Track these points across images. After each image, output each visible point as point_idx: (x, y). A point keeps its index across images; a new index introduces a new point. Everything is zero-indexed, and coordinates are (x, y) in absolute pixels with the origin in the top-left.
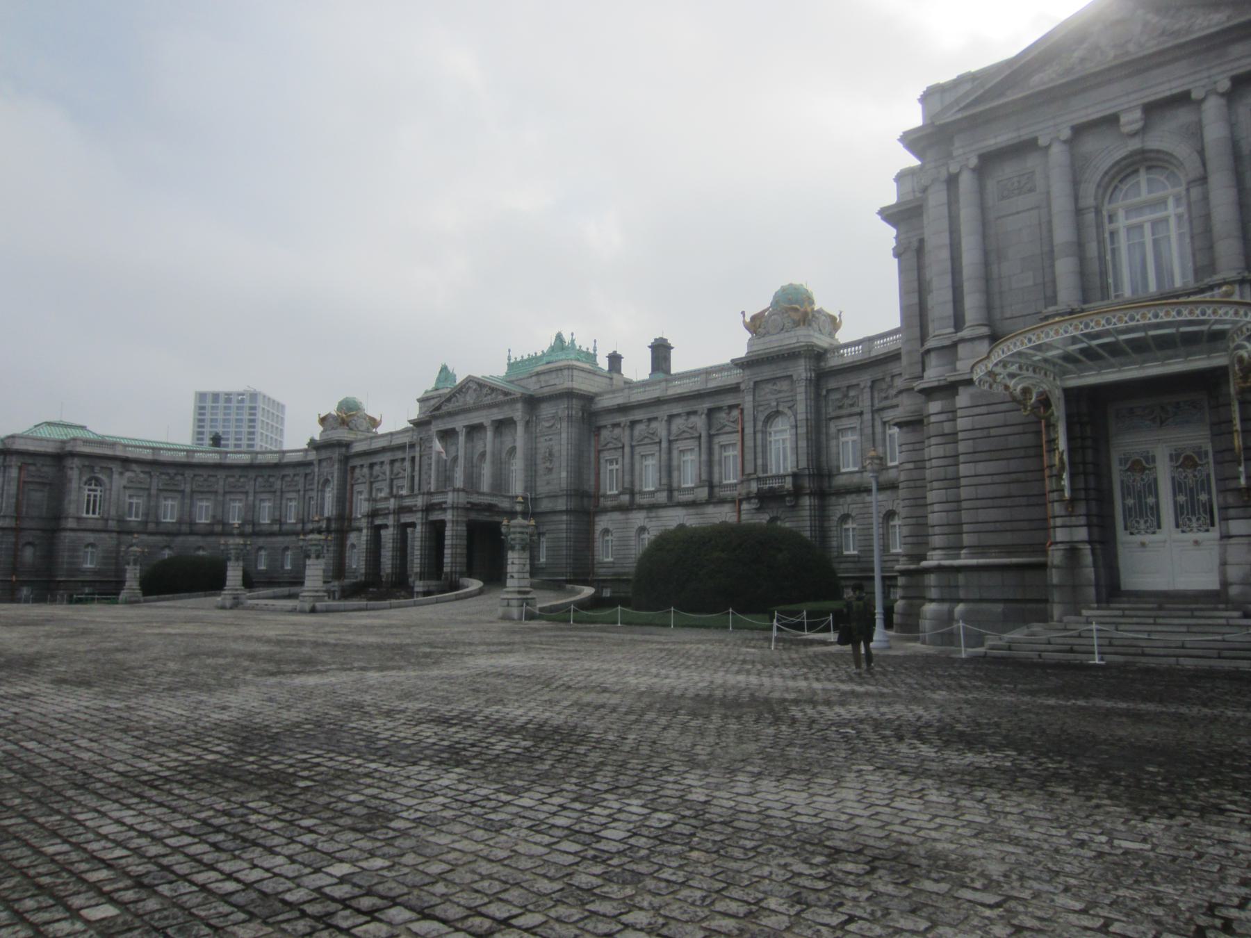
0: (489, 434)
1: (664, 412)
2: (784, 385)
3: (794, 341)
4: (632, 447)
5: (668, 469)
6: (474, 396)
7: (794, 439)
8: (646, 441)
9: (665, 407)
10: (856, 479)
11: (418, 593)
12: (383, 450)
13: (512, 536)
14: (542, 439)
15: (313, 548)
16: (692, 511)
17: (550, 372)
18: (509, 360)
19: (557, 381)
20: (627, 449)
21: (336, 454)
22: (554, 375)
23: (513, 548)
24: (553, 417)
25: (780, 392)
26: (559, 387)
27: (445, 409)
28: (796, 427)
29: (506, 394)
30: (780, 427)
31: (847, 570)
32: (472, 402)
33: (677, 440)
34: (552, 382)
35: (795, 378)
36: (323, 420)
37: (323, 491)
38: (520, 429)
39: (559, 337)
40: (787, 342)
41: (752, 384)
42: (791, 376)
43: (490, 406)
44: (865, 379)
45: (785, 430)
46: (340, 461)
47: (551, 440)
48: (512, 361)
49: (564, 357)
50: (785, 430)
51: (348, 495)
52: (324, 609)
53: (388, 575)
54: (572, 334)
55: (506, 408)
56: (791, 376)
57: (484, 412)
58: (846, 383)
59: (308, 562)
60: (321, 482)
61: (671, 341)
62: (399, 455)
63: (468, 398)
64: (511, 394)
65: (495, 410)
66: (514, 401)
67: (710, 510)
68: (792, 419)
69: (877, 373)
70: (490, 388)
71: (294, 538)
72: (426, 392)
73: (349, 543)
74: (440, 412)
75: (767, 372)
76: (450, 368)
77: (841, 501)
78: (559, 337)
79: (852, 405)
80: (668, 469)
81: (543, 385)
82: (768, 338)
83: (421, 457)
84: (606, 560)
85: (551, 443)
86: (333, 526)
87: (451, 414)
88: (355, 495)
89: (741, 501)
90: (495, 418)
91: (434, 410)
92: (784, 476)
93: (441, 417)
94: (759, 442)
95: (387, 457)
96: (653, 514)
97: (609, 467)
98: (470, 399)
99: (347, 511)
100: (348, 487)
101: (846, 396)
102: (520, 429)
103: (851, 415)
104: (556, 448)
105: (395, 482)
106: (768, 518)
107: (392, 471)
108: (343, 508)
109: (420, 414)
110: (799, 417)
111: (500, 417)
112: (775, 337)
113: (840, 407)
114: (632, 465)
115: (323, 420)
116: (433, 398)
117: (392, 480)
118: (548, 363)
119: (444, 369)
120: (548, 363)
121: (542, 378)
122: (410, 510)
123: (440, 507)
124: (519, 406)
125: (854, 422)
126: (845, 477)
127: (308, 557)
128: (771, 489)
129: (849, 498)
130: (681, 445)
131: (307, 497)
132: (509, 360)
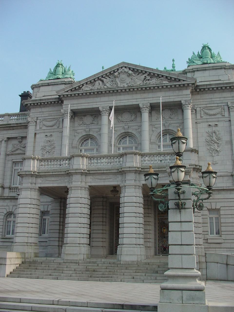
0: (146, 115)
57: (138, 96)
66: (184, 87)
124: (188, 92)
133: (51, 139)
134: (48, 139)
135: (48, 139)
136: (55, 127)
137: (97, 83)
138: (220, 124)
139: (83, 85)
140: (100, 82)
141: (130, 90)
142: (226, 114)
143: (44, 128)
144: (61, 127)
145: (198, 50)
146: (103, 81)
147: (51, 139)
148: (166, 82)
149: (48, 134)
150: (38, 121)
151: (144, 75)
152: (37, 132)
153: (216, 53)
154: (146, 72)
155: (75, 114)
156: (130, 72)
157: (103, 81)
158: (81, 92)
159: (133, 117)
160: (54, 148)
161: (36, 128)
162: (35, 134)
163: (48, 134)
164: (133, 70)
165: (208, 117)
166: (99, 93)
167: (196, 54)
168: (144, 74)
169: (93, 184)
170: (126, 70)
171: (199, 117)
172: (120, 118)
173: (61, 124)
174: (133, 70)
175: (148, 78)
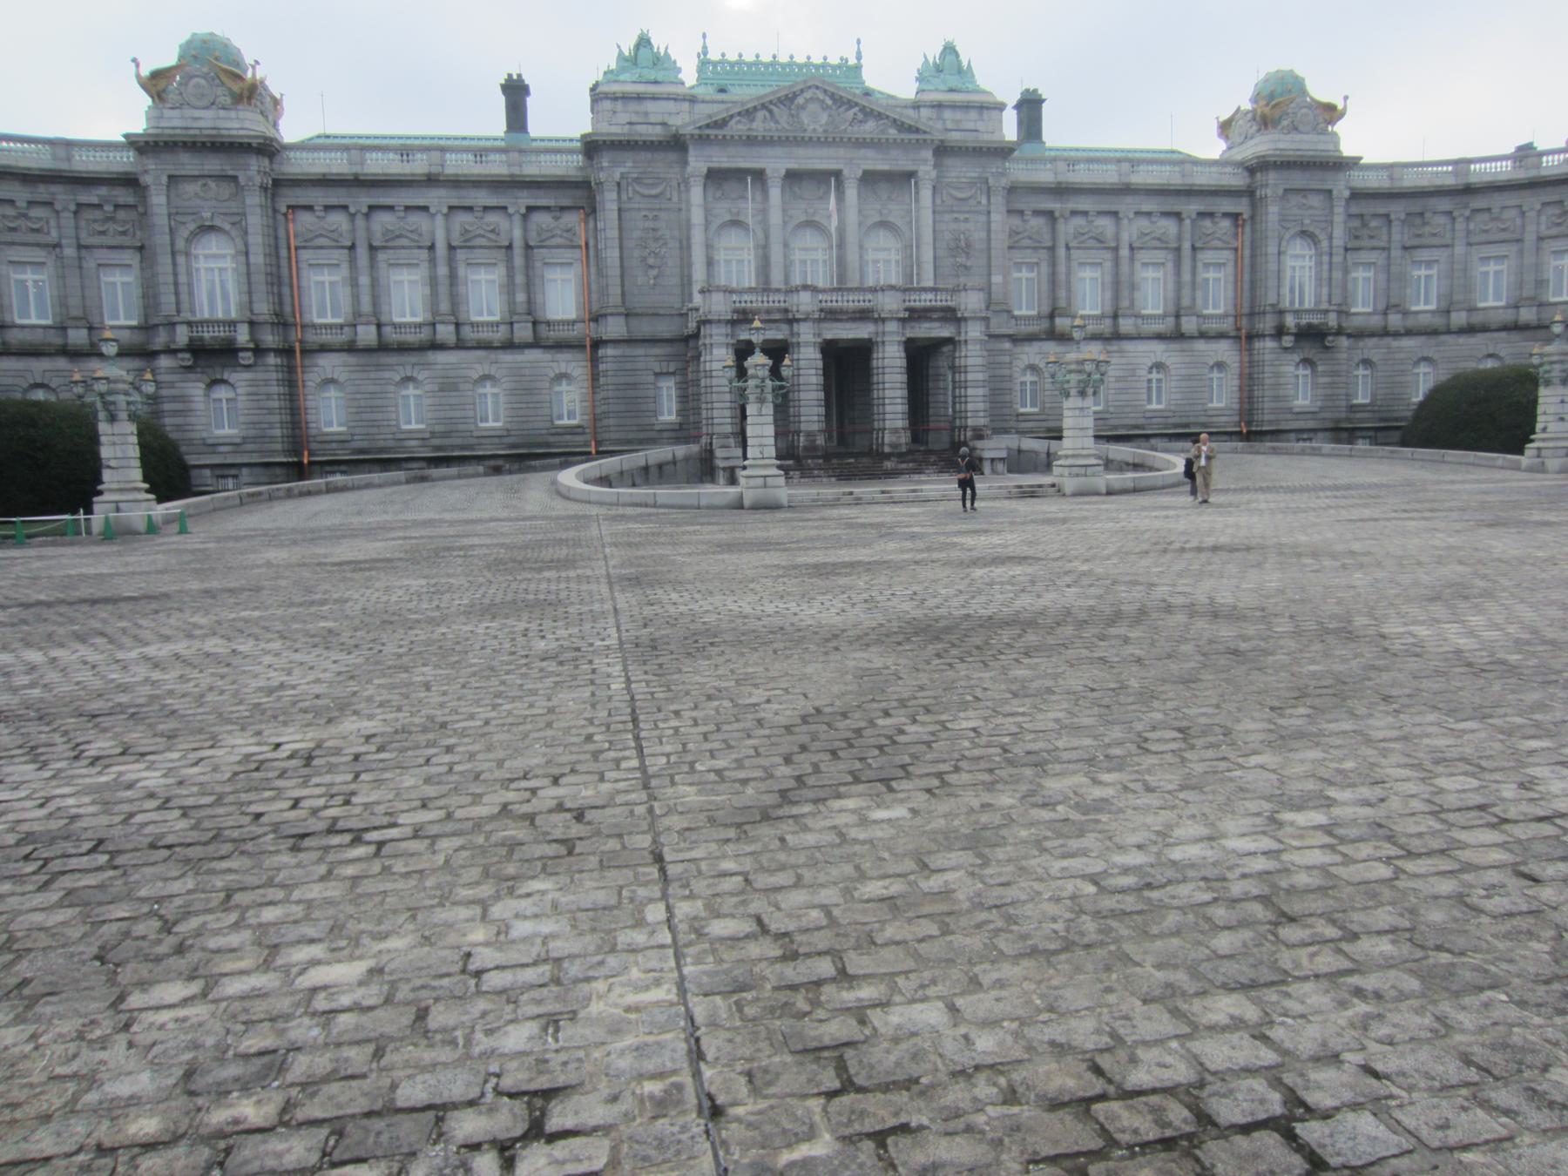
1: (1126, 205)
2: (1315, 201)
4: (1068, 248)
5: (1120, 287)
6: (824, 118)
9: (1129, 199)
10: (1376, 321)
11: (993, 460)
12: (431, 181)
13: (1546, 367)
14: (948, 217)
15: (1073, 378)
16: (1175, 346)
17: (966, 107)
19: (980, 126)
20: (1061, 252)
21: (253, 170)
22: (973, 114)
23: (1548, 383)
24: (972, 184)
25: (1311, 207)
26: (986, 137)
27: (737, 128)
28: (1331, 255)
29: (902, 127)
30: (1298, 252)
31: (1362, 420)
32: (820, 130)
34: (971, 126)
35: (1335, 193)
36: (156, 84)
37: (187, 254)
38: (926, 194)
39: (949, 50)
40: (1321, 147)
41: (1281, 192)
42: (1330, 191)
43: (861, 143)
44: (1397, 210)
45: (1303, 257)
46: (264, 188)
47: (966, 220)
48: (714, 56)
50: (1303, 257)
51: (285, 271)
52: (1130, 485)
53: (809, 434)
54: (859, 42)
55: (894, 153)
56: (1330, 191)
57: (841, 152)
58: (1372, 210)
59: (1067, 404)
60: (184, 233)
62: (482, 198)
63: (805, 118)
64: (917, 131)
65: (870, 153)
66: (922, 144)
67: (1201, 345)
68: (1325, 244)
69: (1416, 206)
70: (863, 109)
71: (61, 363)
73: (312, 378)
74: (727, 131)
75: (1298, 179)
76: (658, 43)
77: (1361, 344)
79: (1371, 237)
80: (1120, 287)
81: (949, 125)
82: (1298, 137)
83: (620, 210)
84: (1022, 410)
86: (269, 339)
87: (751, 141)
88: (305, 273)
90: (870, 166)
91: (708, 126)
92: (1326, 312)
93: (725, 142)
95: (437, 199)
96: (1115, 348)
97: (1016, 275)
98: (815, 120)
99: (288, 309)
100: (284, 253)
101: (1364, 225)
102: (926, 194)
103: (1374, 249)
104: (978, 235)
105: (461, 255)
107: (448, 231)
108: (281, 304)
109: (595, 122)
110: (1335, 242)
111: (883, 167)
112: (1305, 137)
113: (1357, 237)
114: (1068, 274)
115: (156, 84)
116: (655, 98)
117: (451, 248)
118: (951, 90)
119: (643, 42)
120: (951, 90)
121: (948, 114)
122: (863, 315)
123: (950, 315)
124: (928, 154)
125: (1373, 257)
126: (1360, 318)
127: (1068, 396)
128: (1310, 326)
129: (1371, 342)
130: (1143, 256)
131: (90, 264)
134: (651, 224)
137: (761, 114)
139: (732, 117)
141: (828, 141)
142: (984, 201)
144: (675, 199)
145: (934, 53)
146: (770, 112)
148: (893, 132)
150: (624, 183)
152: (624, 206)
153: (965, 64)
154: (857, 104)
155: (716, 177)
156: (830, 102)
157: (770, 112)
158: (727, 131)
163: (650, 215)
164: (832, 96)
166: (768, 142)
167: (931, 61)
168: (851, 107)
170: (821, 95)
173: (675, 193)
174: (832, 96)
175: (860, 116)
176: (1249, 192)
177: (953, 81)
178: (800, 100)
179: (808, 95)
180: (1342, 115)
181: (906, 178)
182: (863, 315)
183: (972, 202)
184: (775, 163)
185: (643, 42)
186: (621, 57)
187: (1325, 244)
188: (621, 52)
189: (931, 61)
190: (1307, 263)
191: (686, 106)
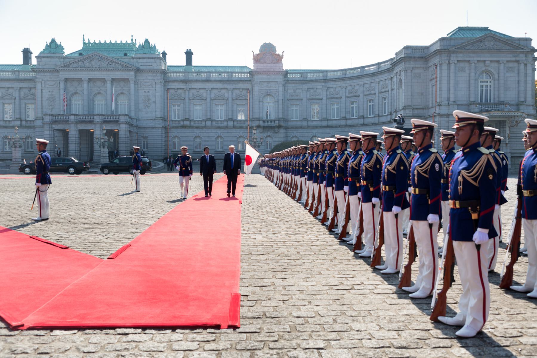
3: (278, 68)
4: (189, 99)
7: (277, 106)
8: (198, 98)
18: (84, 40)
33: (215, 100)
49: (152, 52)
57: (105, 73)
61: (192, 51)
63: (93, 63)
72: (41, 53)
78: (147, 41)
85: (148, 94)
89: (251, 128)
94: (261, 106)
101: (295, 92)
102: (132, 85)
106: (265, 136)
119: (53, 41)
132: (84, 40)
133: (53, 93)
134: (50, 93)
135: (50, 93)
136: (55, 86)
137: (80, 63)
138: (151, 92)
140: (82, 63)
141: (100, 69)
142: (154, 86)
143: (47, 86)
144: (58, 86)
146: (83, 62)
147: (53, 93)
149: (51, 90)
150: (43, 82)
151: (107, 62)
152: (43, 88)
155: (66, 80)
157: (83, 62)
159: (103, 84)
160: (55, 99)
161: (42, 86)
162: (42, 90)
163: (51, 90)
165: (144, 87)
167: (141, 44)
169: (81, 128)
171: (139, 86)
172: (95, 84)
175: (110, 63)
176: (249, 81)
177: (146, 51)
178: (91, 59)
179: (93, 57)
180: (282, 57)
181: (126, 80)
182: (91, 122)
183: (150, 87)
184: (85, 75)
185: (53, 41)
186: (47, 45)
187: (276, 99)
188: (47, 44)
189: (141, 44)
190: (272, 105)
191: (62, 60)
